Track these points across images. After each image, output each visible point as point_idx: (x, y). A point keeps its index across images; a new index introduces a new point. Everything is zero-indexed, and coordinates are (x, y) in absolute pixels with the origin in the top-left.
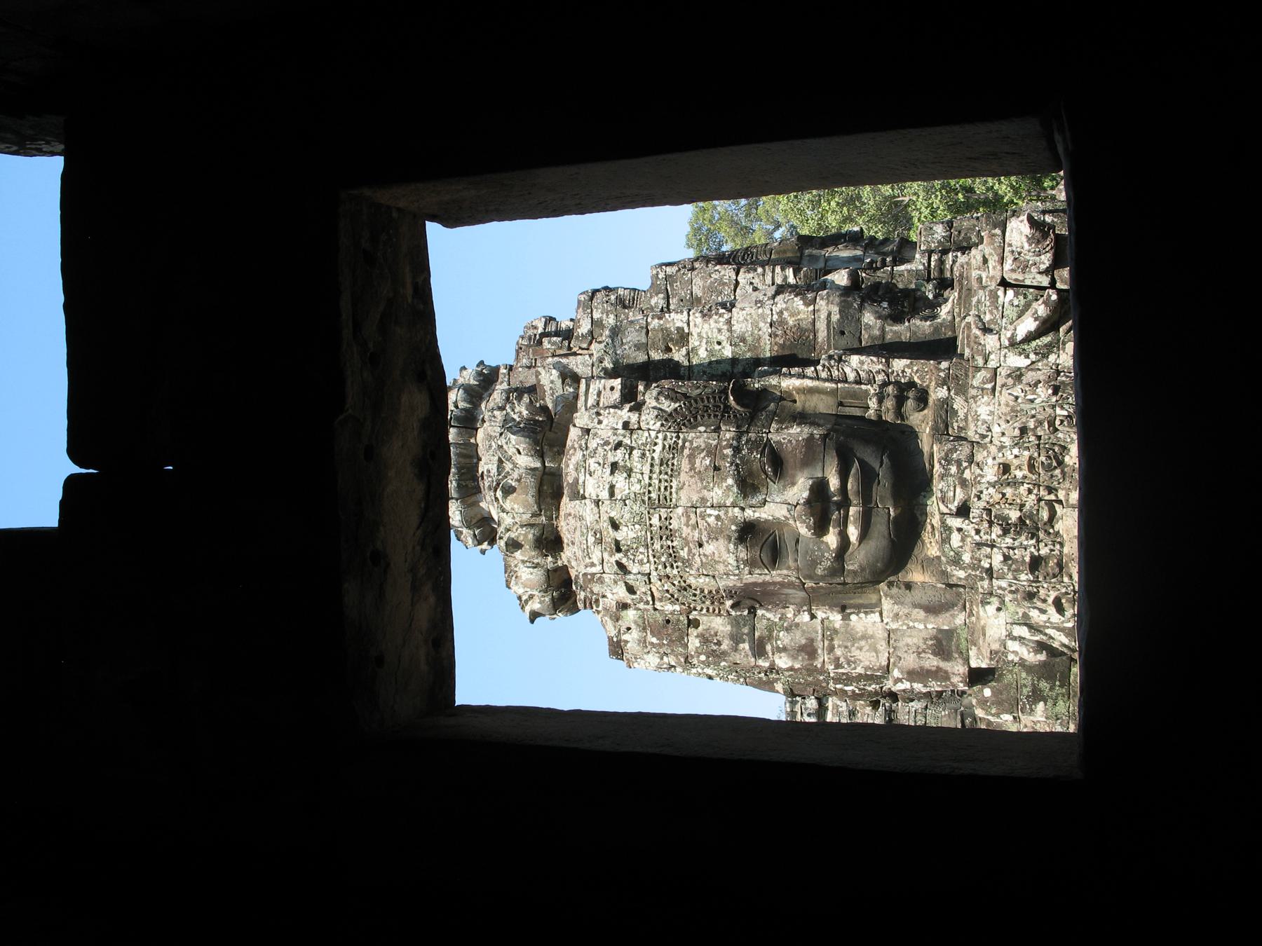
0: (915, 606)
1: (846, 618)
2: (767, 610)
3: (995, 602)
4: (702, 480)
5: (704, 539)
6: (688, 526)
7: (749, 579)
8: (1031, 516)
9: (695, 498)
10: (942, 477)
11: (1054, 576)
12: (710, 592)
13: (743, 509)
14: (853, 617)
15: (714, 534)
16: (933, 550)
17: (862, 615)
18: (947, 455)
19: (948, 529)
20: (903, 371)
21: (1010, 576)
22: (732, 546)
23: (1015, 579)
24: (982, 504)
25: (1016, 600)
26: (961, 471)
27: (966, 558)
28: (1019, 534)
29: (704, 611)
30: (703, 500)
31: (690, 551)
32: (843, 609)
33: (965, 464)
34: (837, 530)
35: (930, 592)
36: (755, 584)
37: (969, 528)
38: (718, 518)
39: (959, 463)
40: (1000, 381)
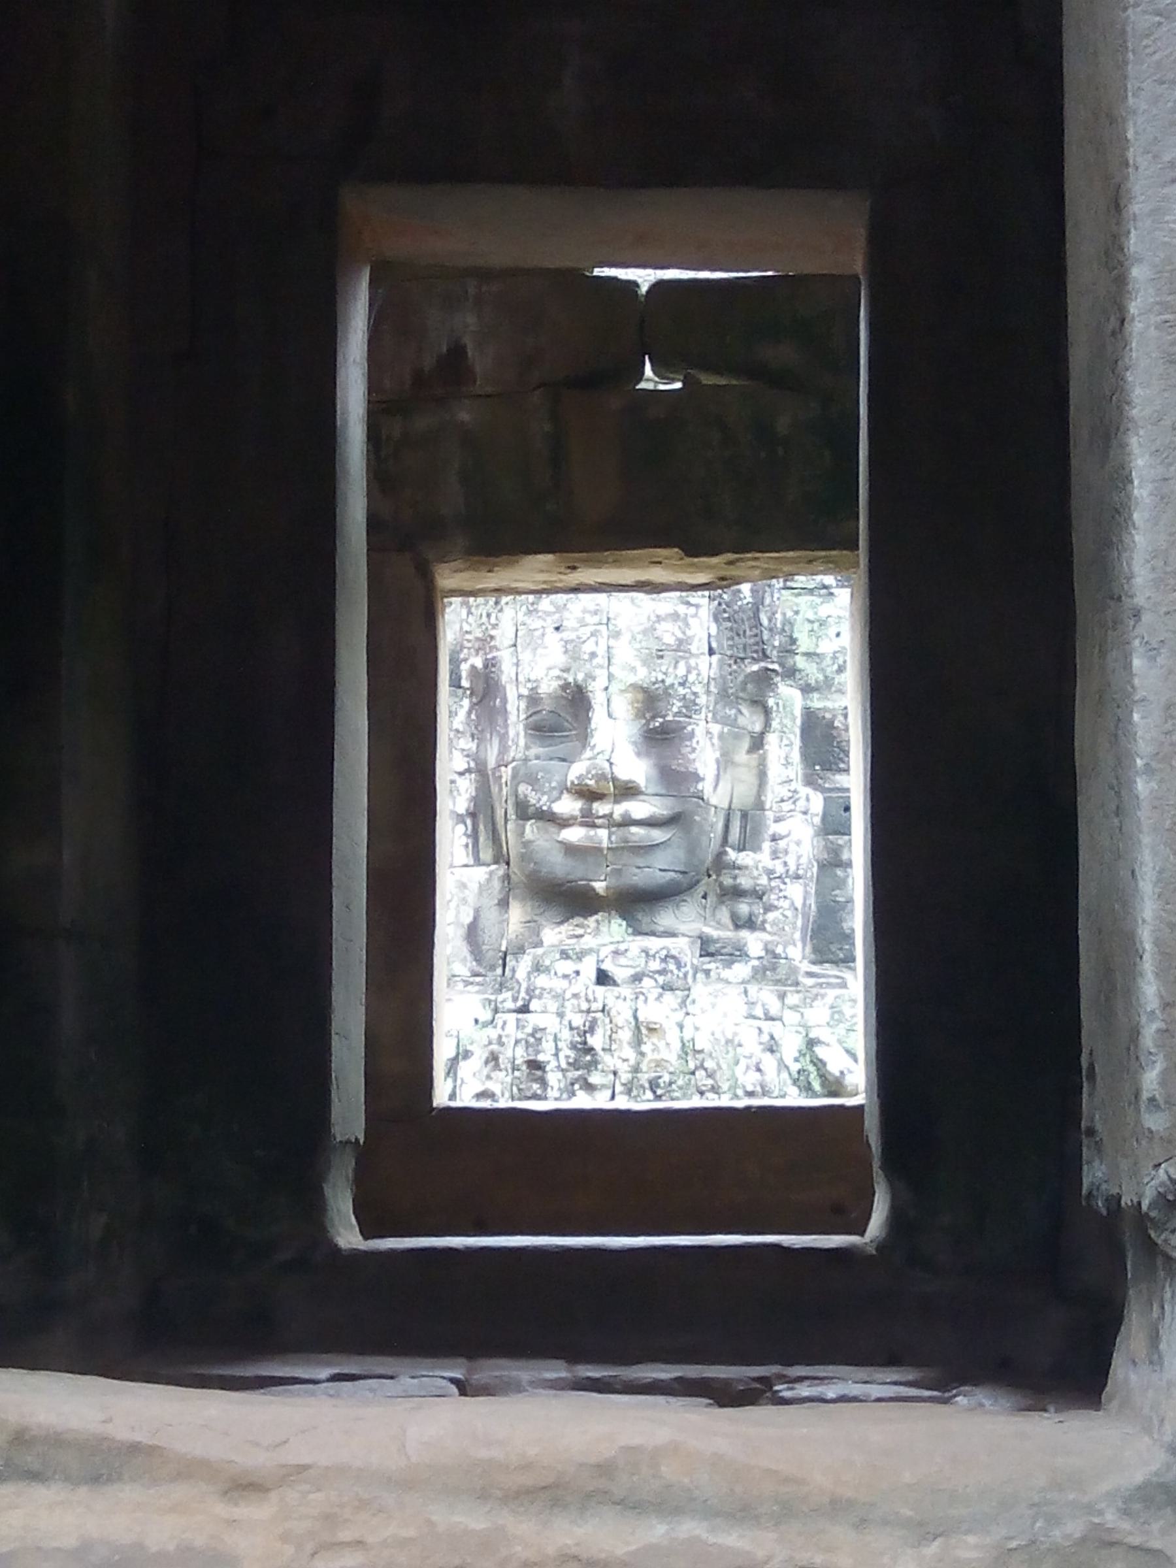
0: (477, 911)
2: (469, 713)
3: (486, 1015)
4: (645, 632)
5: (566, 635)
6: (585, 611)
7: (511, 693)
8: (595, 1063)
9: (620, 623)
10: (646, 952)
11: (519, 1090)
12: (492, 637)
13: (606, 689)
15: (572, 650)
16: (554, 935)
18: (673, 957)
19: (580, 956)
20: (785, 897)
21: (520, 1036)
22: (557, 672)
23: (517, 1042)
24: (610, 1002)
25: (490, 1043)
26: (652, 975)
27: (542, 981)
28: (573, 1046)
29: (466, 627)
30: (617, 635)
31: (548, 614)
32: (473, 815)
33: (661, 979)
34: (577, 813)
36: (505, 701)
37: (578, 986)
38: (593, 655)
39: (662, 972)
40: (767, 1026)
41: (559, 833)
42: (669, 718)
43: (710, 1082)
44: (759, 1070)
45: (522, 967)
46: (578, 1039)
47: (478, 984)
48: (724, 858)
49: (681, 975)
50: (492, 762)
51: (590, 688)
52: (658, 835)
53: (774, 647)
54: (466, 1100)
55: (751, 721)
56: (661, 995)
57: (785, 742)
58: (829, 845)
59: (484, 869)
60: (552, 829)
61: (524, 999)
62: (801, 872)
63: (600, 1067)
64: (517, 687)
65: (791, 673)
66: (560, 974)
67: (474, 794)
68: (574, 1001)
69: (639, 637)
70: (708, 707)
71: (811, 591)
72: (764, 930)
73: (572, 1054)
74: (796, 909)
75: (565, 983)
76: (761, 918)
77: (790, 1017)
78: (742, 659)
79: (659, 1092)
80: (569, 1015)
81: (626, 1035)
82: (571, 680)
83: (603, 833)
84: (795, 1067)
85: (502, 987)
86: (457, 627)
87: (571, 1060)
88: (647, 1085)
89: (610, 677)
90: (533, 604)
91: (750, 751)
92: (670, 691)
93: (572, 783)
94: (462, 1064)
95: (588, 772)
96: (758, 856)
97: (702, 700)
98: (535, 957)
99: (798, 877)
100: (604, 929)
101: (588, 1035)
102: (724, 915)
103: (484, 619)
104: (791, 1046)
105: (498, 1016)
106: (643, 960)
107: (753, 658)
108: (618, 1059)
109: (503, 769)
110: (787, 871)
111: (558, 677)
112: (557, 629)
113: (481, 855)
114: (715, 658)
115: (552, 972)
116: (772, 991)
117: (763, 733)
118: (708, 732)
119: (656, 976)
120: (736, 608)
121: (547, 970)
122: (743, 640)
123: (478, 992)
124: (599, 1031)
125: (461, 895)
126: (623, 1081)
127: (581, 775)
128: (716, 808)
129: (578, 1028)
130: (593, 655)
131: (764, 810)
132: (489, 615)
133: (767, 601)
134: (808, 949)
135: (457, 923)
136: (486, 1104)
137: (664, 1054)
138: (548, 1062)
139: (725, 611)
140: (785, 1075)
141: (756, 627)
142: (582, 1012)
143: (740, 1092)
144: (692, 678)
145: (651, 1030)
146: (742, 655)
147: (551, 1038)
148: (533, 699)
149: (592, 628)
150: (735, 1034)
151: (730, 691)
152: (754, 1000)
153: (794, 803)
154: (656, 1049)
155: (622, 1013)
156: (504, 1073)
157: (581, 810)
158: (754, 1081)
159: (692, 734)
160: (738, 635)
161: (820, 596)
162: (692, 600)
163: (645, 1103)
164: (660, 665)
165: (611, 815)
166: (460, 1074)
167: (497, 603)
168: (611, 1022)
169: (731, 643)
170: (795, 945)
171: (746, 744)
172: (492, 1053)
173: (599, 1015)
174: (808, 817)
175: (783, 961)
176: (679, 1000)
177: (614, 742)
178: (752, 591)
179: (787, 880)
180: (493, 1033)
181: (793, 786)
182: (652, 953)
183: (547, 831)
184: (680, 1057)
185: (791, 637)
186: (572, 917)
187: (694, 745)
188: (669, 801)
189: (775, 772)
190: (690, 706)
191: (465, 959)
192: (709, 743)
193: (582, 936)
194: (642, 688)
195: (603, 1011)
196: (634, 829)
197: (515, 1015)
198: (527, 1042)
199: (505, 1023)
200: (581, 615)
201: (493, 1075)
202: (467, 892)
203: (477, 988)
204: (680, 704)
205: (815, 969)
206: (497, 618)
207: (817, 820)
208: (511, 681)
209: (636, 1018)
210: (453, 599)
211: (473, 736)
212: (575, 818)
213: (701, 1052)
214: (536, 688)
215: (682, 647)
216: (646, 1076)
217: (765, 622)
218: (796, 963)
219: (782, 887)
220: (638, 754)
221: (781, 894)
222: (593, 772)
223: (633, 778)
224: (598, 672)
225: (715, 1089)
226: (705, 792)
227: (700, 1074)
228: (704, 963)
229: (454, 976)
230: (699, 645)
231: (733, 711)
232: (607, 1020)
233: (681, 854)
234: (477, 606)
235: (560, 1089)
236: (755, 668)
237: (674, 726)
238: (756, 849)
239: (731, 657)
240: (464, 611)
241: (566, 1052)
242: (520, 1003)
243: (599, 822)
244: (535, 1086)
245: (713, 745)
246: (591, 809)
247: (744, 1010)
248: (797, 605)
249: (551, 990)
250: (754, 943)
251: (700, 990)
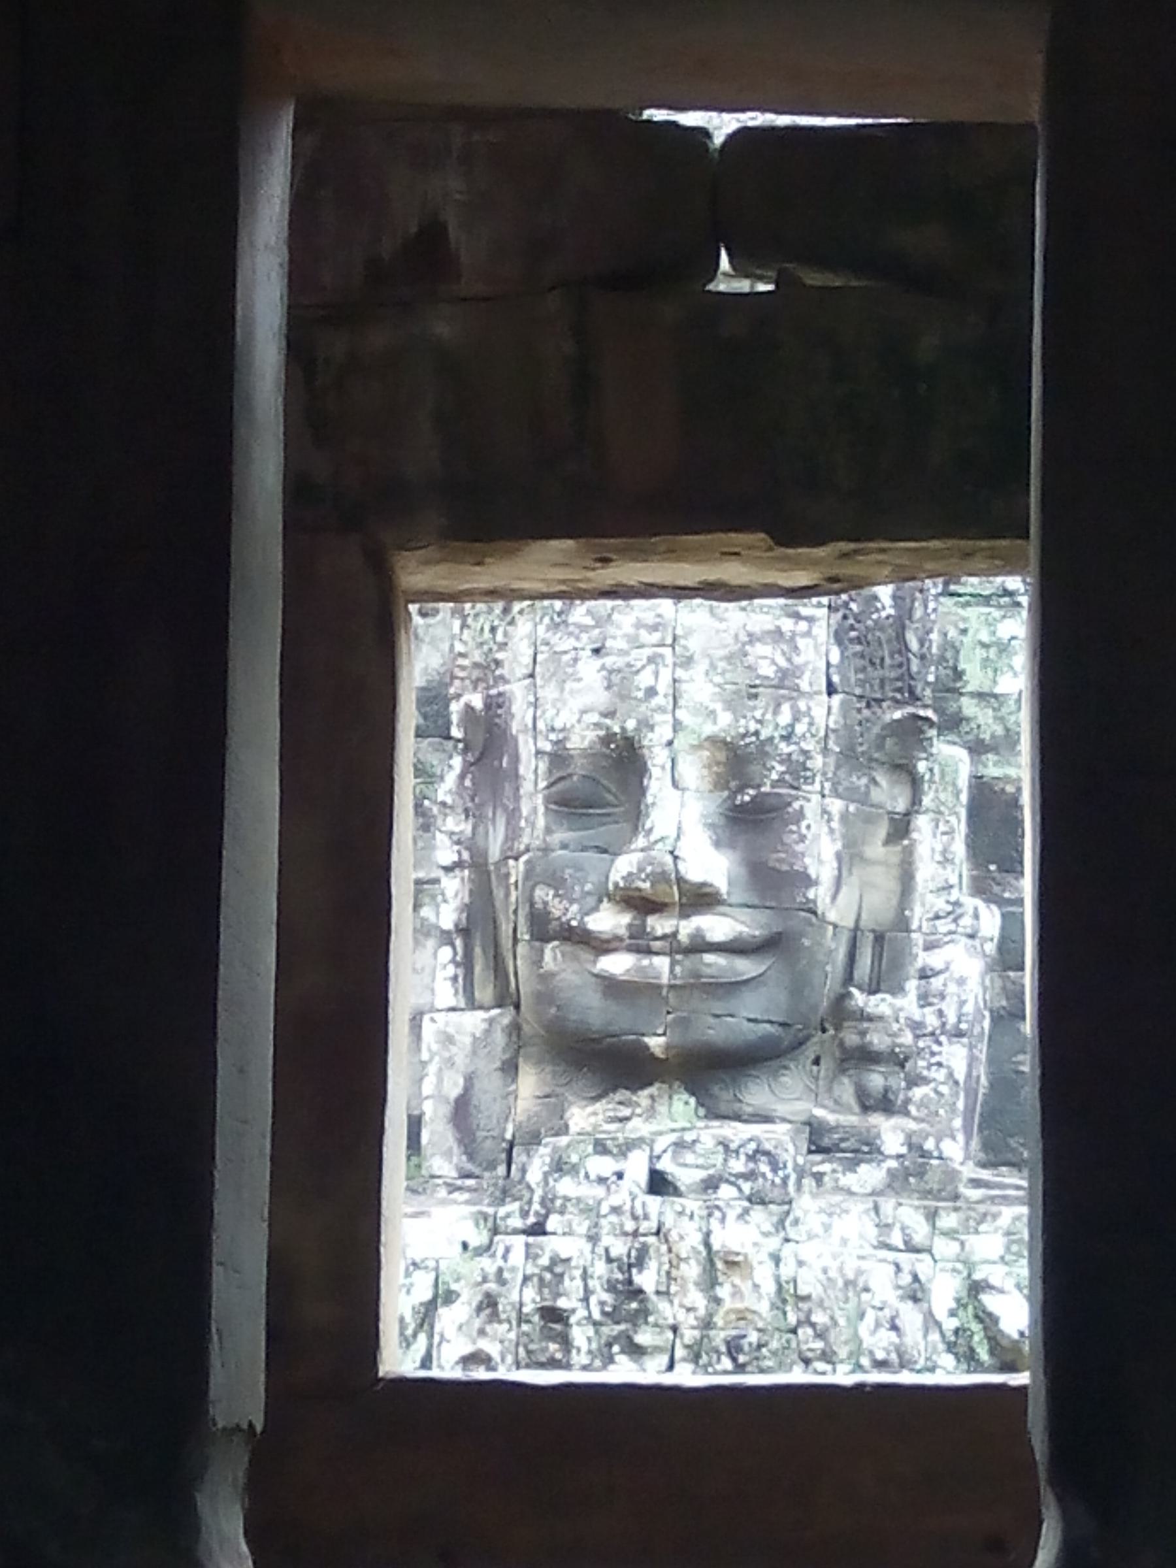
0: (469, 1080)
1: (446, 938)
2: (462, 777)
3: (478, 1238)
4: (729, 658)
5: (609, 661)
6: (639, 625)
7: (526, 747)
8: (644, 1313)
9: (693, 644)
10: (724, 1144)
11: (529, 1352)
12: (498, 663)
13: (670, 743)
14: (446, 953)
15: (618, 682)
16: (582, 1117)
18: (767, 1153)
19: (626, 1148)
20: (939, 1064)
21: (530, 1269)
22: (594, 718)
23: (526, 1279)
24: (669, 1220)
25: (485, 1280)
26: (733, 1180)
27: (566, 1186)
28: (611, 1287)
29: (459, 647)
30: (687, 662)
31: (584, 628)
32: (465, 931)
33: (747, 1187)
34: (623, 932)
35: (497, 1108)
36: (516, 759)
38: (651, 692)
39: (750, 1176)
40: (905, 1259)
41: (595, 962)
42: (766, 789)
43: (819, 1345)
44: (894, 1328)
45: (536, 1167)
46: (620, 1276)
47: (469, 1190)
48: (847, 1001)
49: (778, 1181)
50: (495, 852)
51: (645, 743)
52: (746, 967)
53: (928, 684)
54: (447, 1369)
55: (890, 794)
56: (746, 1211)
57: (942, 827)
58: (1009, 985)
59: (481, 1014)
60: (585, 955)
61: (537, 1213)
62: (964, 1026)
63: (651, 1319)
64: (535, 738)
65: (953, 723)
66: (593, 1177)
67: (467, 900)
68: (613, 1218)
69: (722, 665)
70: (824, 774)
71: (986, 600)
72: (907, 1114)
73: (607, 1297)
74: (956, 1083)
75: (600, 1191)
76: (901, 1097)
77: (945, 1248)
78: (879, 701)
79: (742, 1359)
80: (606, 1240)
81: (692, 1271)
82: (617, 729)
83: (662, 963)
84: (950, 1324)
85: (504, 1195)
86: (446, 647)
87: (608, 1309)
88: (723, 1349)
89: (677, 726)
90: (559, 614)
91: (890, 840)
92: (768, 748)
93: (616, 885)
94: (442, 1311)
95: (641, 870)
96: (899, 1002)
97: (817, 762)
98: (555, 1149)
99: (960, 1034)
100: (662, 1108)
101: (634, 1271)
102: (846, 1090)
103: (487, 634)
104: (944, 1292)
105: (497, 1238)
106: (720, 1158)
107: (897, 701)
108: (682, 1308)
109: (511, 862)
110: (944, 1024)
111: (597, 725)
112: (597, 651)
113: (477, 994)
114: (837, 699)
115: (582, 1174)
116: (917, 1208)
117: (907, 814)
118: (825, 811)
119: (740, 1182)
120: (870, 623)
121: (574, 1170)
122: (880, 673)
123: (467, 1202)
124: (652, 1265)
125: (447, 1055)
126: (687, 1341)
127: (630, 874)
128: (835, 926)
129: (619, 1259)
130: (651, 692)
131: (908, 930)
132: (493, 630)
133: (918, 614)
134: (975, 1143)
135: (439, 1097)
136: (481, 1374)
137: (750, 1302)
138: (573, 1311)
139: (852, 628)
140: (935, 1337)
141: (900, 652)
142: (626, 1234)
143: (865, 1361)
144: (800, 728)
145: (731, 1264)
146: (878, 696)
147: (578, 1273)
148: (559, 758)
149: (648, 652)
150: (860, 1272)
151: (860, 749)
152: (890, 1221)
153: (955, 921)
154: (737, 1293)
155: (688, 1237)
156: (506, 1326)
157: (630, 926)
158: (885, 1344)
159: (800, 815)
160: (872, 664)
161: (999, 607)
162: (804, 611)
163: (721, 1375)
164: (754, 708)
165: (675, 934)
166: (437, 1329)
167: (506, 611)
168: (670, 1250)
169: (861, 676)
170: (954, 1138)
171: (882, 830)
172: (488, 1295)
173: (652, 1240)
174: (977, 943)
175: (935, 1162)
176: (775, 1219)
177: (682, 826)
178: (894, 597)
179: (943, 1039)
180: (489, 1265)
181: (955, 895)
182: (733, 1146)
183: (576, 958)
184: (773, 1306)
185: (955, 668)
186: (614, 1089)
187: (804, 831)
188: (763, 916)
189: (926, 872)
190: (798, 771)
191: (450, 1149)
192: (825, 829)
193: (627, 1119)
195: (658, 1233)
196: (709, 958)
197: (522, 1239)
198: (541, 1279)
199: (507, 1250)
200: (631, 631)
201: (488, 1329)
202: (454, 1049)
203: (466, 1196)
204: (783, 769)
205: (985, 1174)
206: (506, 634)
207: (991, 948)
208: (525, 730)
209: (707, 1245)
210: (441, 605)
211: (466, 811)
212: (619, 939)
213: (807, 1298)
214: (565, 739)
215: (785, 682)
216: (722, 1334)
217: (914, 645)
218: (957, 1166)
219: (935, 1048)
220: (717, 844)
221: (934, 1060)
222: (649, 869)
223: (709, 880)
224: (658, 718)
225: (827, 1356)
226: (819, 904)
227: (805, 1332)
228: (814, 1164)
229: (433, 1177)
230: (812, 680)
231: (864, 781)
232: (664, 1248)
233: (782, 997)
234: (477, 615)
235: (590, 1352)
236: (898, 715)
237: (773, 801)
238: (897, 990)
239: (861, 697)
240: (457, 624)
241: (601, 1295)
242: (532, 1220)
243: (657, 945)
244: (553, 1347)
245: (832, 831)
246: (644, 925)
247: (872, 1233)
248: (965, 620)
249: (579, 1200)
250: (891, 1135)
251: (806, 1205)
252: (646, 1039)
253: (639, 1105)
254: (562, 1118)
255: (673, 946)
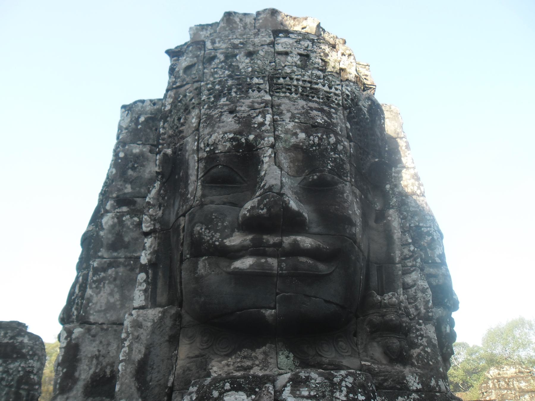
0: (149, 348)
17: (144, 286)
38: (262, 124)
60: (223, 263)
89: (277, 138)
103: (176, 121)
125: (136, 334)
194: (301, 148)
202: (141, 331)
252: (263, 311)
253: (256, 358)
254: (205, 370)
255: (278, 251)
